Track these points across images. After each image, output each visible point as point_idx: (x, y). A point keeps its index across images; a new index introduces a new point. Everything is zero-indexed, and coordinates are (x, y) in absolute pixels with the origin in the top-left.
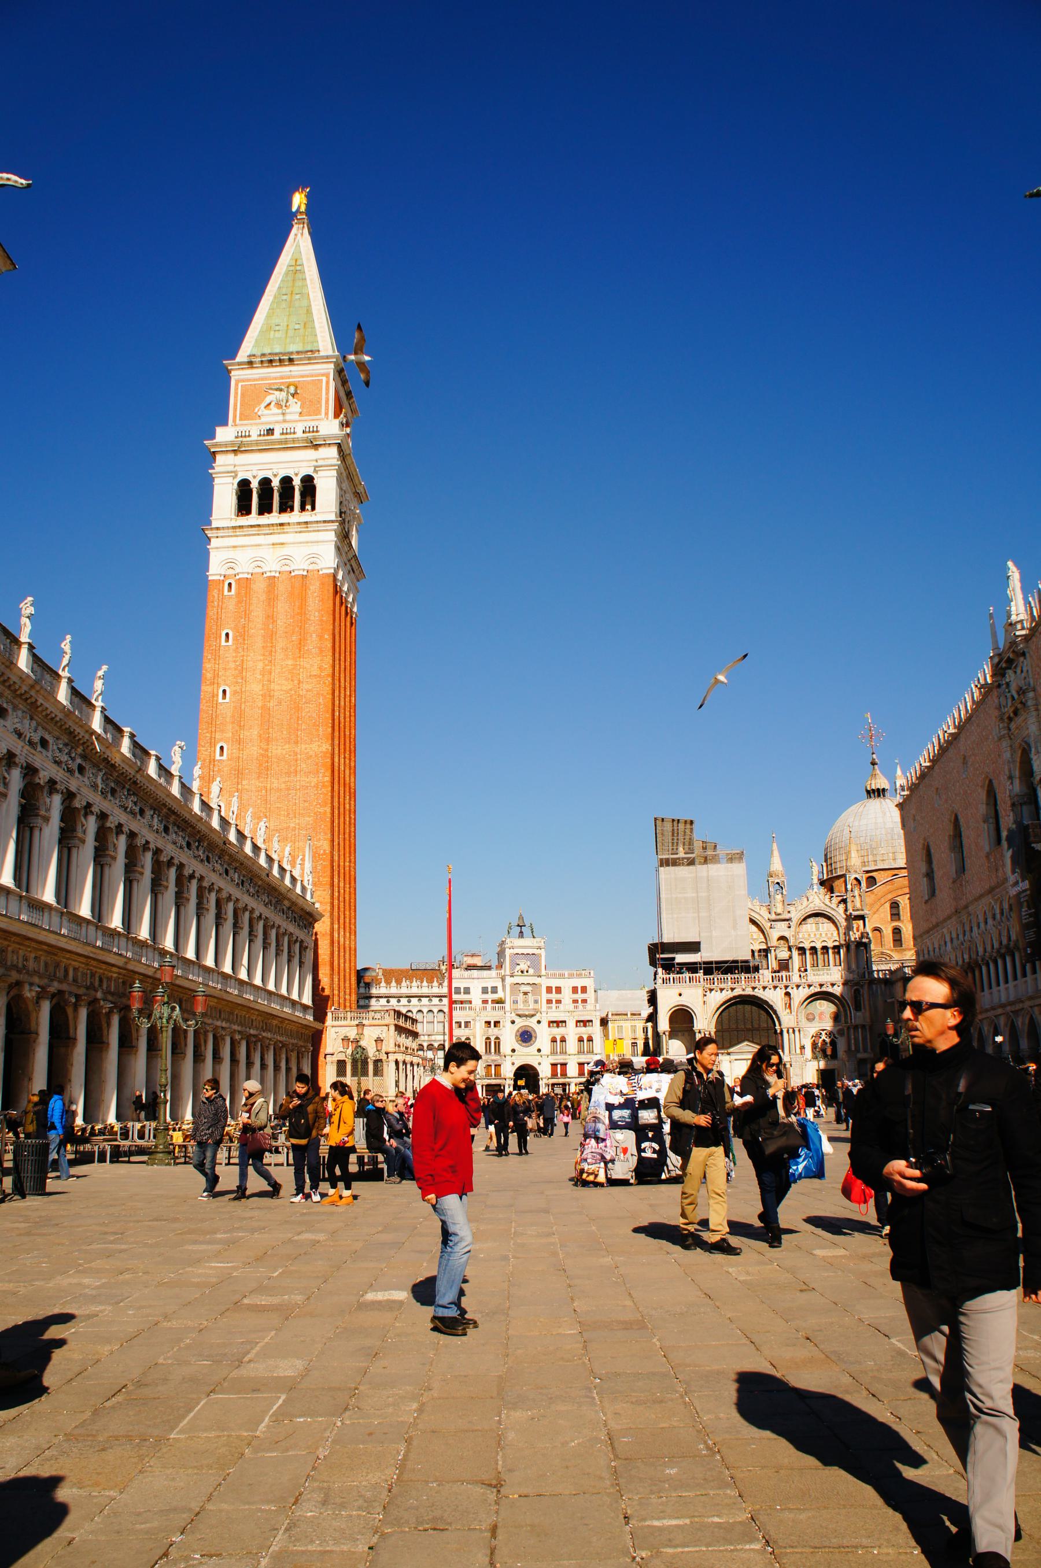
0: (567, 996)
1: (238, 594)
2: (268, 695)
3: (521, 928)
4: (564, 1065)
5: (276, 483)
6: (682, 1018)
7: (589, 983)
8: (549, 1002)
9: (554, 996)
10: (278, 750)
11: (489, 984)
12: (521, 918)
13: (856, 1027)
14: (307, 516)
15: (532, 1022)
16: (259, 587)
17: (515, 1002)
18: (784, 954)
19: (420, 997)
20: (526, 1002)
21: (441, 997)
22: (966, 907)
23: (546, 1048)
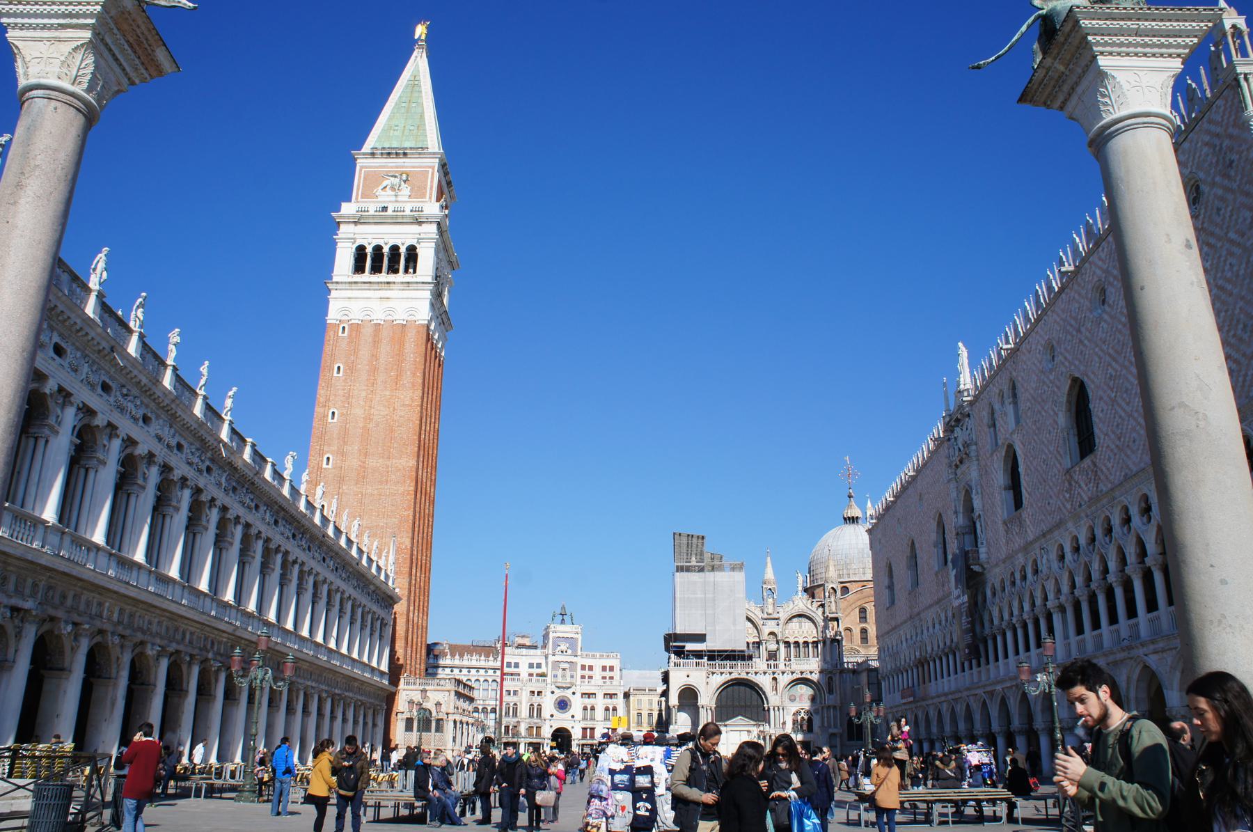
0: (597, 673)
1: (350, 336)
2: (368, 418)
3: (563, 617)
4: (592, 729)
5: (386, 250)
6: (689, 697)
7: (616, 663)
8: (583, 677)
9: (587, 673)
10: (372, 462)
11: (535, 661)
12: (563, 608)
13: (829, 707)
14: (409, 278)
15: (568, 693)
16: (367, 332)
17: (555, 676)
18: (773, 647)
19: (478, 669)
20: (564, 676)
21: (495, 669)
22: (918, 614)
23: (579, 715)
